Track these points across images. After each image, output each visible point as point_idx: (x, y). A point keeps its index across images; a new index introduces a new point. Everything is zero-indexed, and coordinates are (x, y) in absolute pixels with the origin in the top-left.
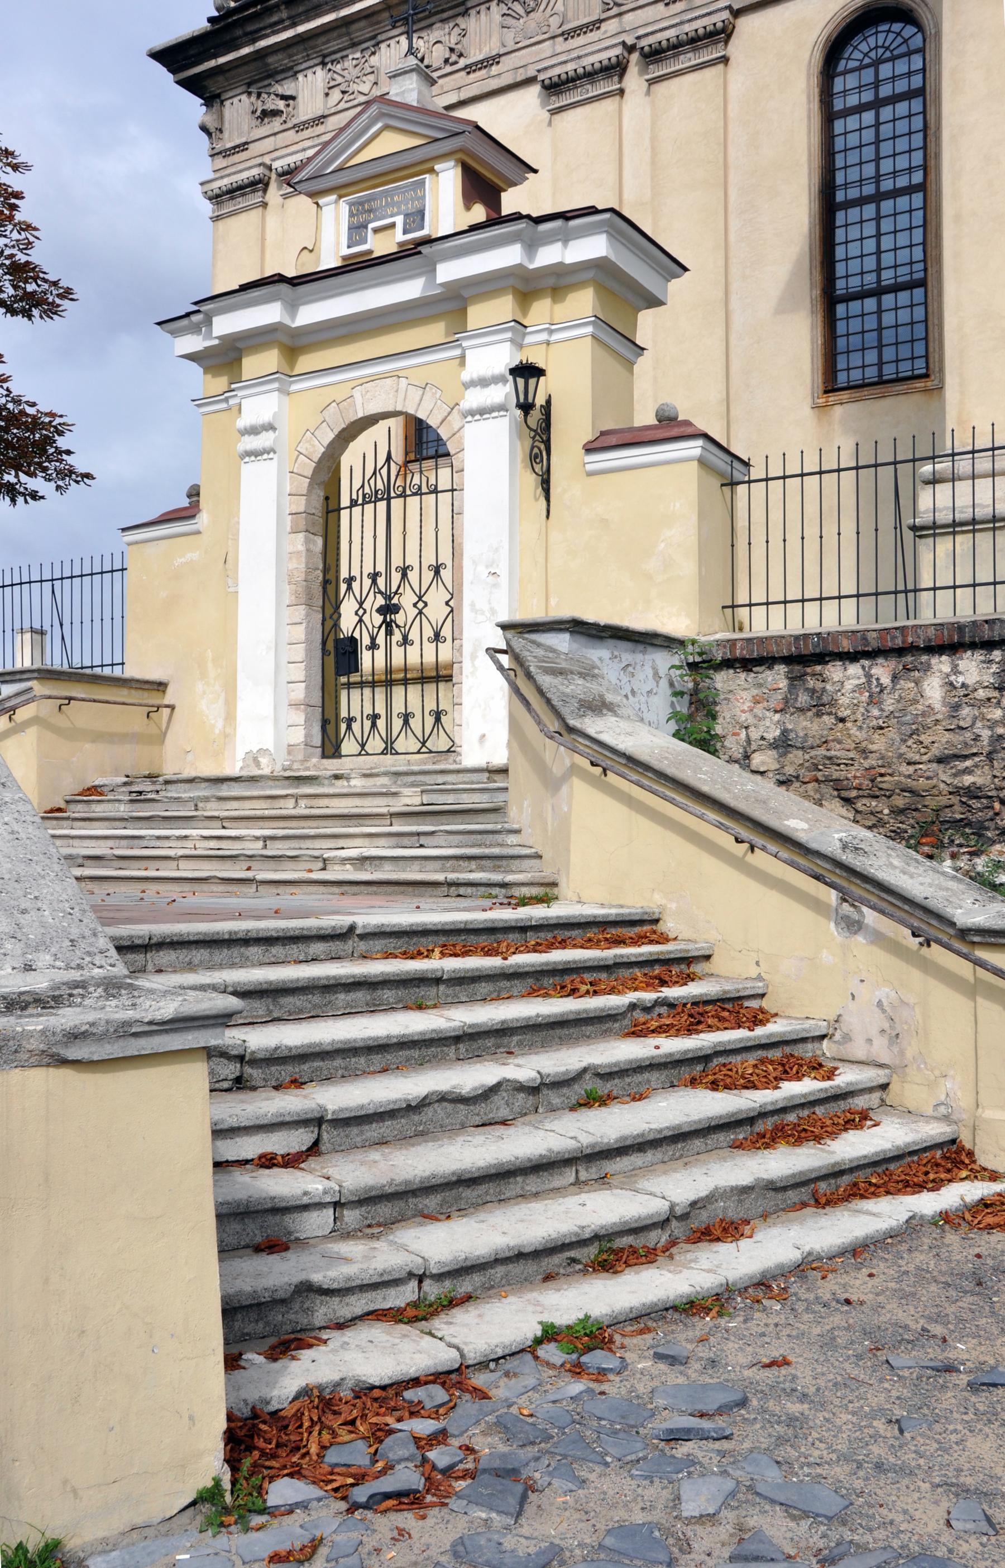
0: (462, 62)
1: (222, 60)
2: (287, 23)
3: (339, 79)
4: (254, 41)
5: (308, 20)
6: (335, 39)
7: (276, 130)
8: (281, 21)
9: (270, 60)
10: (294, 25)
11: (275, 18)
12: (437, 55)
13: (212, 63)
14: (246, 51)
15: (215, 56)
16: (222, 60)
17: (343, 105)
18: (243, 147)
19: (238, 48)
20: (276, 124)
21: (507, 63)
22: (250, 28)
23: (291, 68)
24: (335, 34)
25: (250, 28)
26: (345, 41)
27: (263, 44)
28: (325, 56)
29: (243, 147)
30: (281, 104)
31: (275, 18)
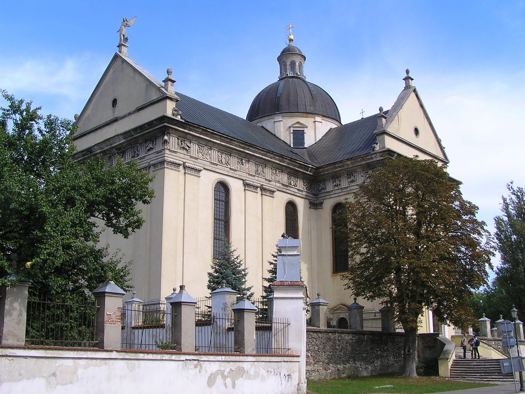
0: (229, 166)
1: (179, 129)
4: (189, 131)
9: (188, 136)
10: (200, 134)
12: (223, 160)
13: (177, 128)
14: (187, 131)
15: (178, 127)
16: (179, 129)
18: (176, 152)
19: (185, 129)
20: (185, 152)
21: (238, 173)
27: (191, 133)
29: (176, 152)
30: (188, 148)
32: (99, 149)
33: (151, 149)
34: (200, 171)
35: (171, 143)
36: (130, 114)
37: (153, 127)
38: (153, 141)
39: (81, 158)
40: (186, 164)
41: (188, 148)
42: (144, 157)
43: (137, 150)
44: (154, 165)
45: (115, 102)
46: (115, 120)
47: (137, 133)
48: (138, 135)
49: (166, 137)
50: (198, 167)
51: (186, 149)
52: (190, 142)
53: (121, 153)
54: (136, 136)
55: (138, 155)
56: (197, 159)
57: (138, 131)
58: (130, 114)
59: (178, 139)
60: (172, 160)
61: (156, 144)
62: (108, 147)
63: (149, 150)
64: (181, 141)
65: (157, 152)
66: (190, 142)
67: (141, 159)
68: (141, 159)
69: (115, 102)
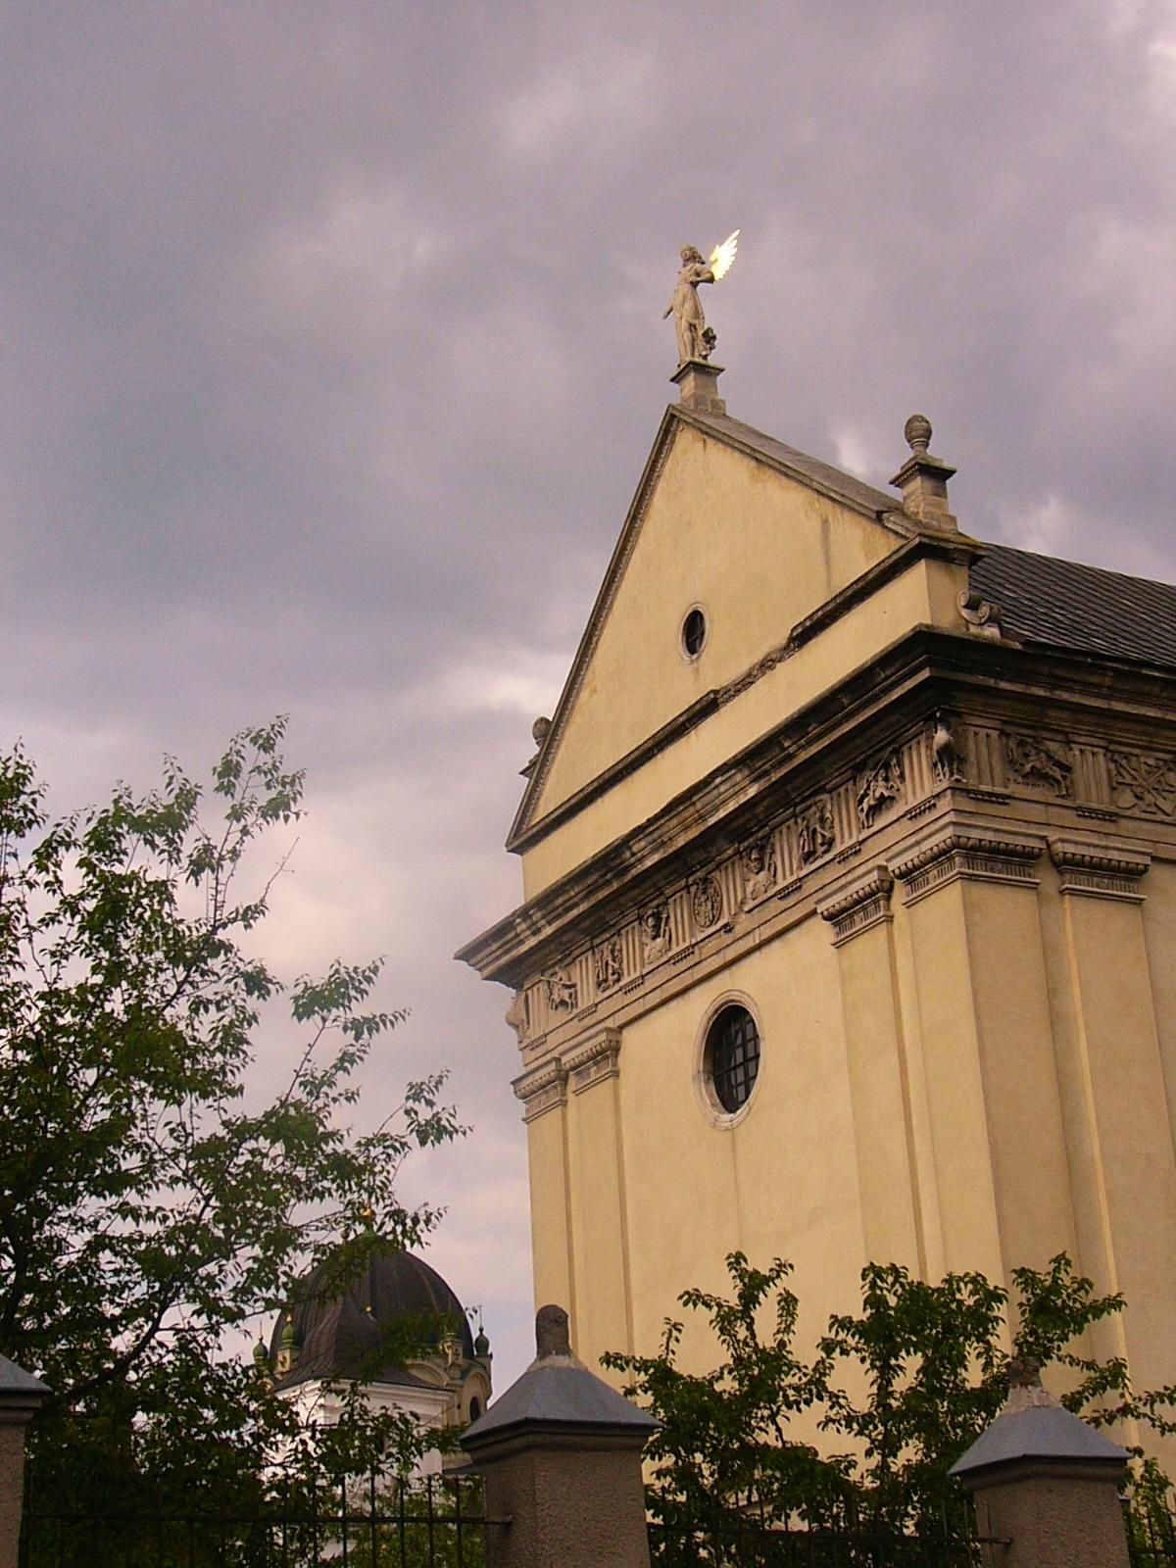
1: (1003, 685)
2: (1105, 691)
3: (1128, 780)
4: (1054, 687)
5: (1127, 701)
6: (1136, 733)
7: (1051, 800)
8: (1100, 686)
9: (1053, 713)
10: (1108, 697)
11: (1094, 679)
13: (991, 682)
15: (998, 676)
16: (1003, 685)
17: (1137, 813)
18: (1002, 799)
19: (1029, 683)
22: (1060, 672)
23: (1066, 733)
24: (1140, 728)
25: (1060, 672)
26: (1143, 740)
27: (1065, 696)
28: (1111, 742)
29: (1002, 799)
30: (1057, 773)
31: (1094, 679)
32: (655, 850)
33: (883, 803)
34: (1132, 874)
35: (972, 758)
36: (767, 665)
37: (876, 698)
38: (887, 766)
39: (583, 907)
40: (1059, 847)
41: (1057, 773)
42: (856, 850)
43: (822, 820)
44: (908, 875)
45: (694, 629)
46: (708, 706)
47: (810, 743)
48: (813, 750)
49: (941, 736)
50: (1125, 857)
51: (1055, 777)
52: (1068, 743)
53: (750, 849)
54: (804, 756)
55: (829, 843)
56: (1112, 817)
57: (814, 730)
58: (767, 665)
59: (1003, 733)
60: (989, 836)
61: (902, 776)
62: (693, 833)
63: (875, 810)
64: (1021, 744)
65: (914, 814)
66: (1068, 743)
67: (843, 857)
68: (843, 857)
69: (694, 629)
